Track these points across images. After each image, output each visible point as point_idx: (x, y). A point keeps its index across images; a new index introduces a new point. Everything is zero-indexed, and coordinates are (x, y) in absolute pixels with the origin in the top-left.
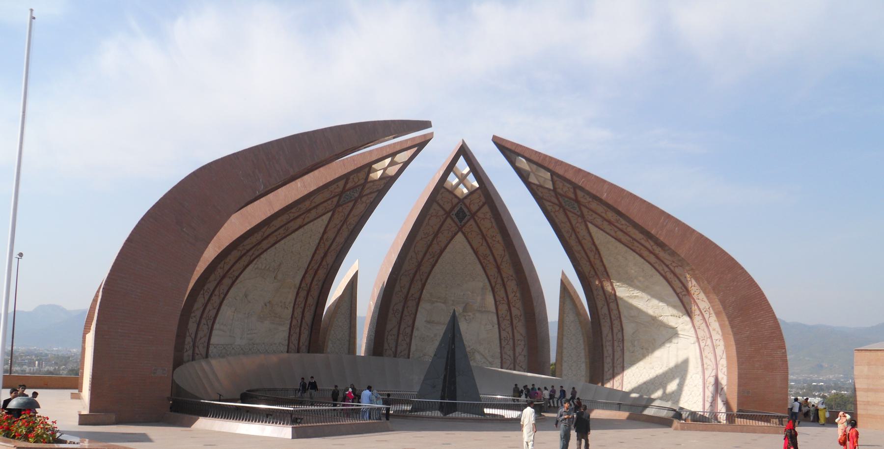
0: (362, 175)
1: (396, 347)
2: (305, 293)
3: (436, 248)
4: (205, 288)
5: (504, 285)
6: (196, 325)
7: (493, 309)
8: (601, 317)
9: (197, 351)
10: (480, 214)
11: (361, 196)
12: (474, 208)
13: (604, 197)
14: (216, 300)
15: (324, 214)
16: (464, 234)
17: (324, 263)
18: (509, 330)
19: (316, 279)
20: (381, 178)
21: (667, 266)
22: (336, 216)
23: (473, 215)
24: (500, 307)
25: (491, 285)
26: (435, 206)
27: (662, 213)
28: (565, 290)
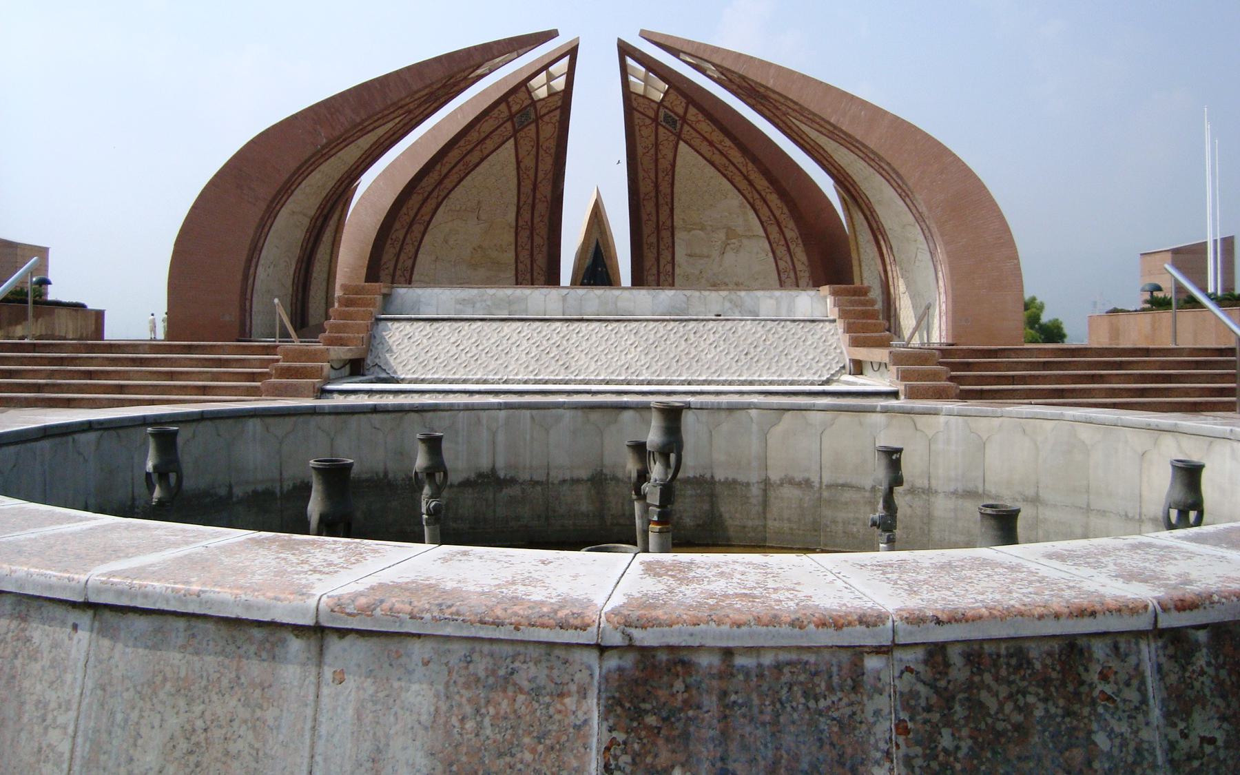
0: (522, 94)
2: (528, 232)
3: (664, 164)
5: (765, 202)
7: (761, 232)
11: (539, 118)
12: (680, 111)
13: (770, 84)
14: (410, 249)
15: (503, 143)
16: (686, 142)
17: (538, 195)
19: (536, 214)
20: (550, 95)
23: (684, 119)
24: (769, 229)
26: (636, 115)
27: (845, 94)
28: (843, 201)
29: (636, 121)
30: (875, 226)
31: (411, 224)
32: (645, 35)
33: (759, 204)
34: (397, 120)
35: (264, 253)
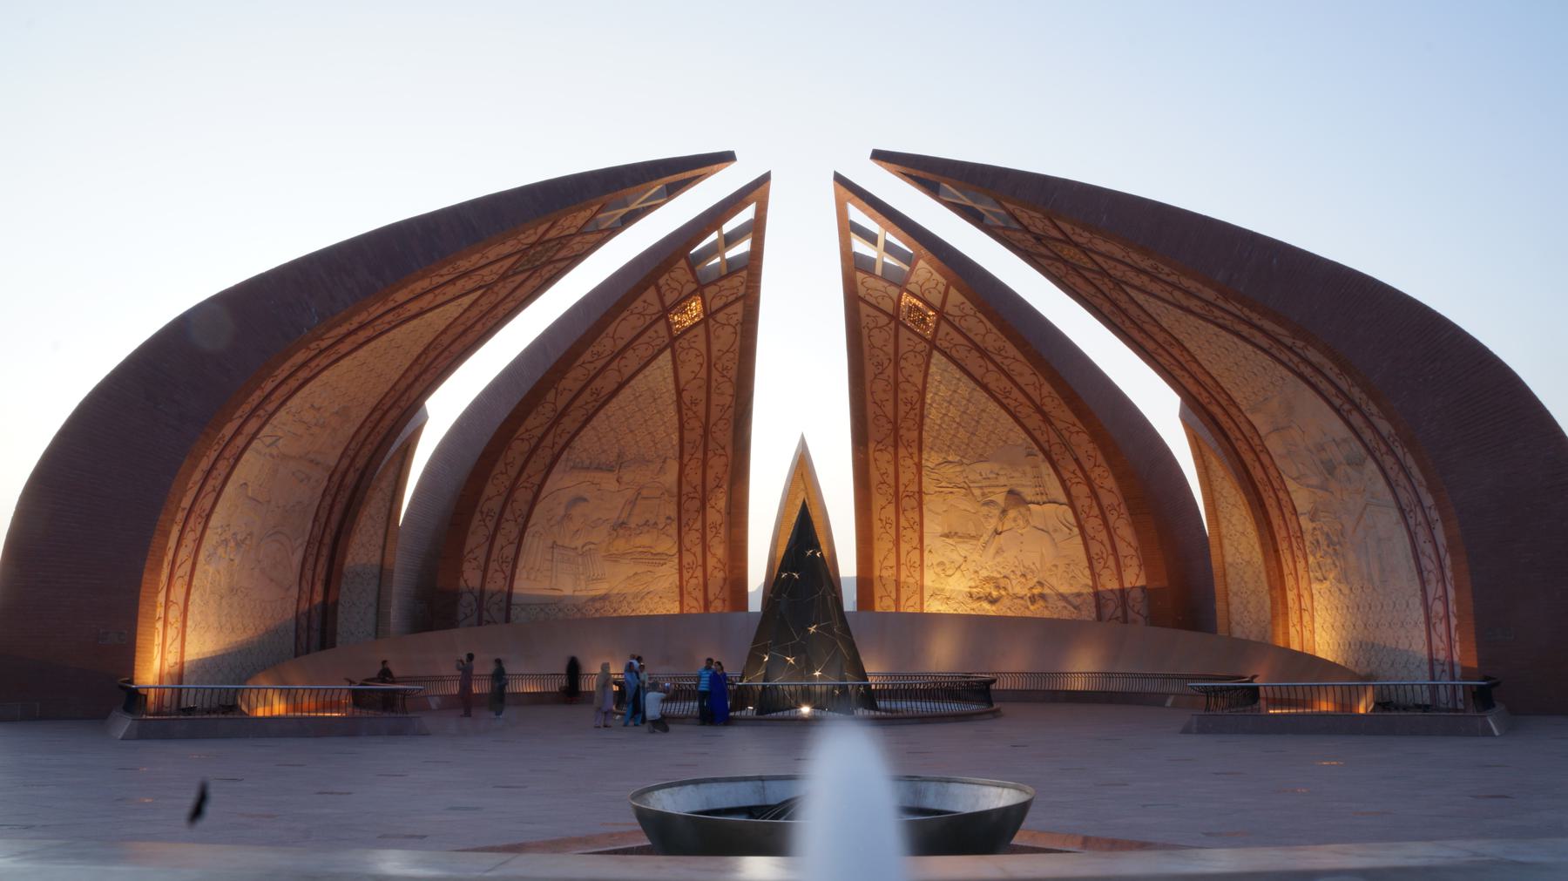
0: (680, 272)
1: (898, 590)
3: (908, 392)
4: (485, 510)
6: (479, 574)
8: (1260, 487)
9: (486, 616)
10: (949, 308)
12: (936, 299)
14: (510, 528)
15: (654, 357)
16: (944, 353)
17: (712, 445)
18: (1103, 536)
21: (1290, 349)
22: (683, 356)
23: (941, 314)
24: (1074, 490)
25: (1042, 449)
29: (864, 321)
30: (1258, 474)
31: (512, 489)
32: (878, 156)
33: (1056, 450)
34: (467, 301)
35: (214, 522)
